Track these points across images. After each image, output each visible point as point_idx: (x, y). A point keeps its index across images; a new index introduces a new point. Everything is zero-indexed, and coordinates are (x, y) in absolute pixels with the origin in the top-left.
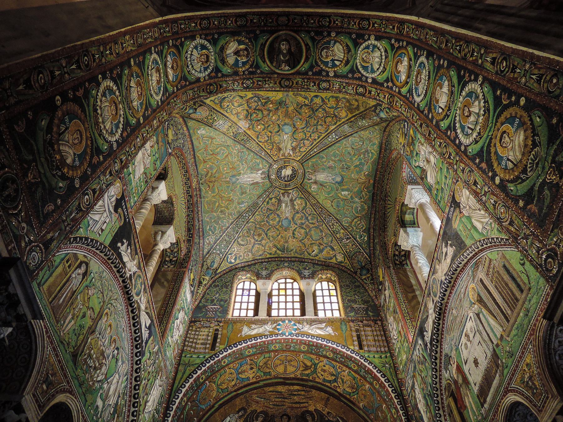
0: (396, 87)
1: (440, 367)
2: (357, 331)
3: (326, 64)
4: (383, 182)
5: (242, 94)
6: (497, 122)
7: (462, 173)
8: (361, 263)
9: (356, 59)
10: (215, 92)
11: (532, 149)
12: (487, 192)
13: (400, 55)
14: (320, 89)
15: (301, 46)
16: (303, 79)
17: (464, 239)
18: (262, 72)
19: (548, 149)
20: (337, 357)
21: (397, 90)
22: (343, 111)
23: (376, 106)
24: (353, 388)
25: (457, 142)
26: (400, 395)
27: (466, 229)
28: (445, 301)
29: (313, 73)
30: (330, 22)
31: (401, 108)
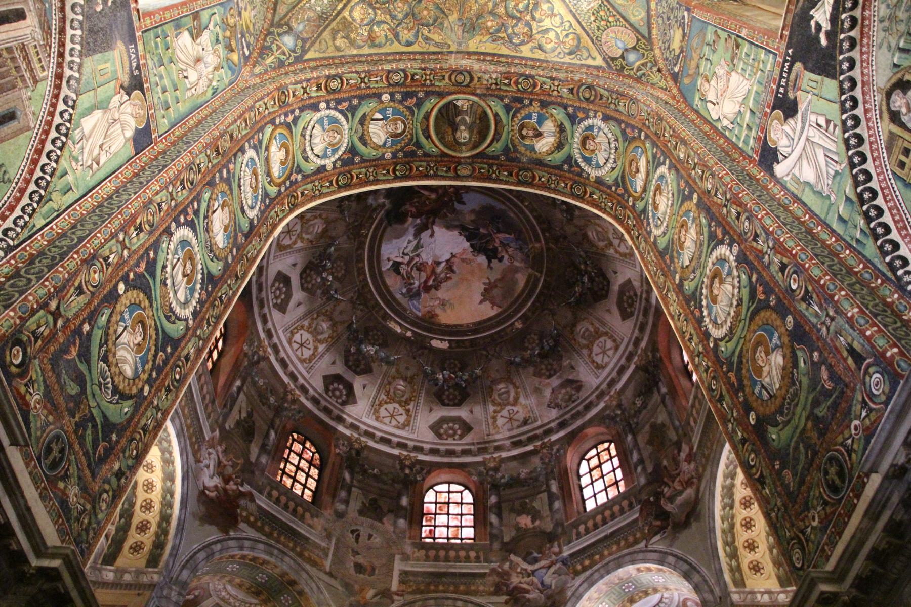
3: (396, 112)
5: (538, 55)
6: (156, 329)
10: (583, 84)
13: (284, 170)
14: (404, 71)
15: (437, 134)
16: (432, 85)
18: (501, 98)
19: (103, 413)
21: (277, 122)
22: (359, 21)
23: (304, 51)
25: (182, 219)
29: (416, 96)
30: (394, 171)
31: (266, 104)
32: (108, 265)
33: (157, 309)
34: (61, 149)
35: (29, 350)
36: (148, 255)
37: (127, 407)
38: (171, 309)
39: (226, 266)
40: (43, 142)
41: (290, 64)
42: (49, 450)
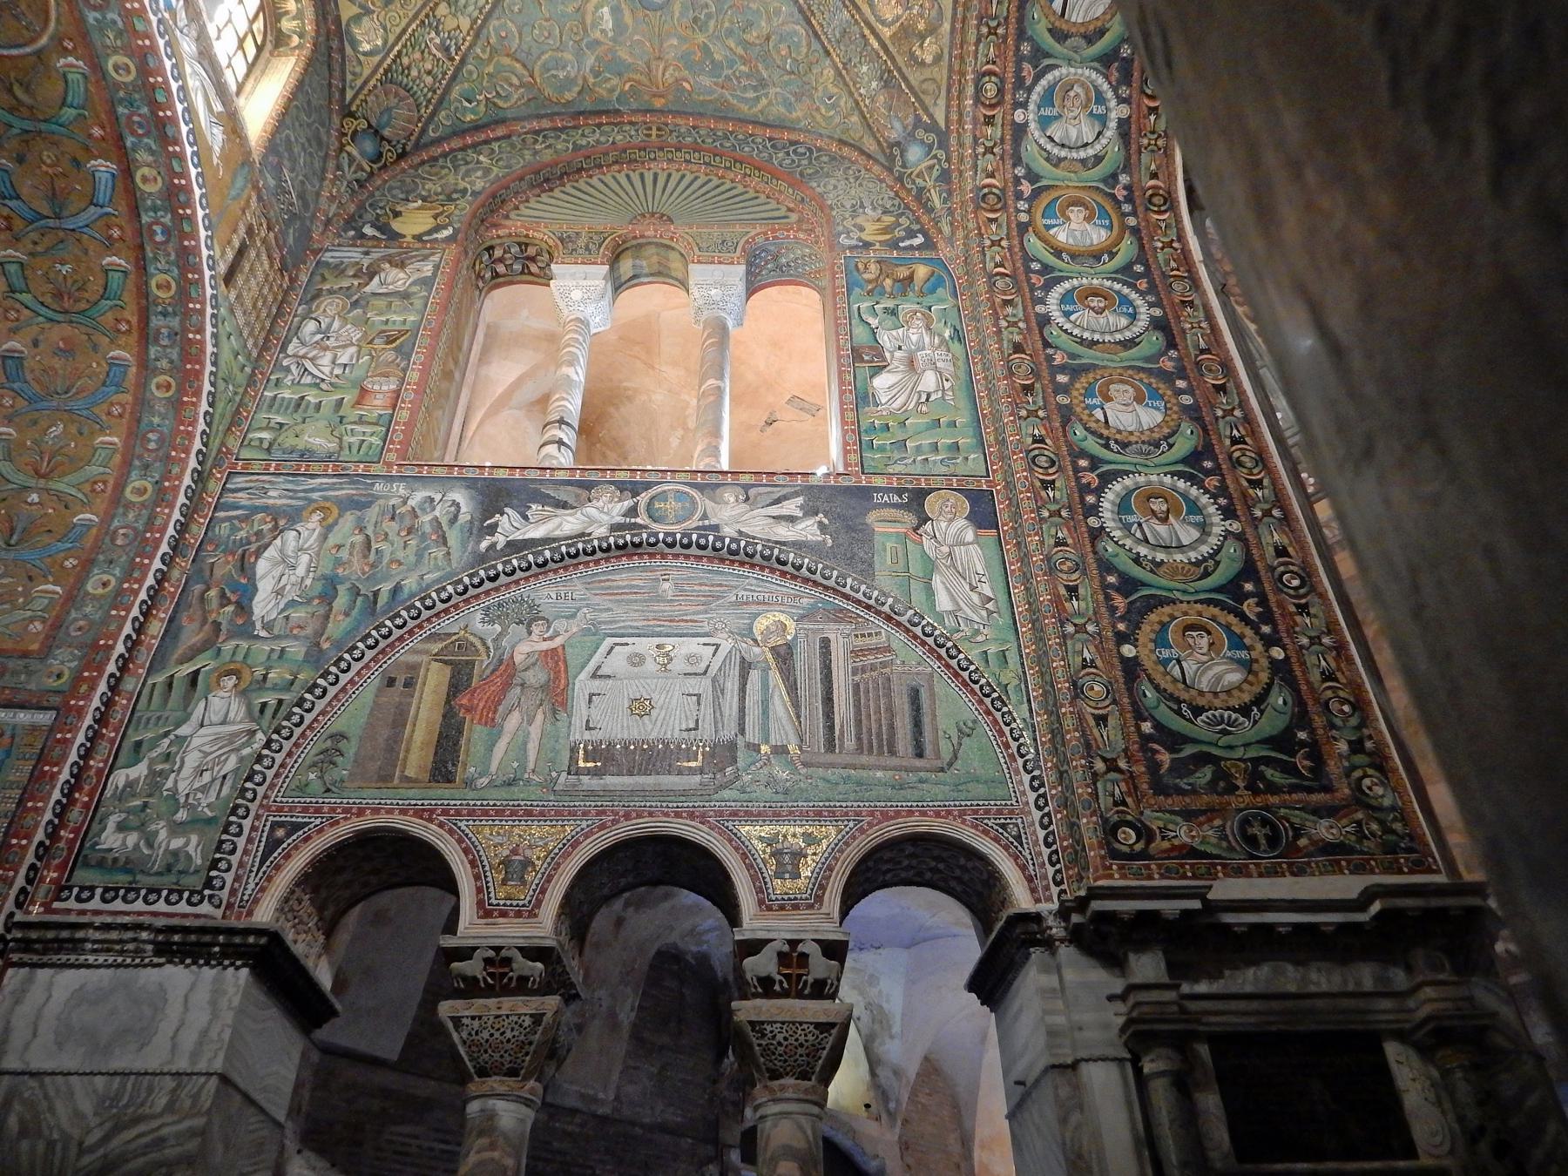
0: (1029, 211)
1: (477, 597)
2: (250, 231)
4: (678, 149)
6: (1208, 602)
7: (1052, 541)
8: (388, 124)
9: (1070, 62)
11: (1234, 710)
12: (1087, 633)
13: (1104, 214)
17: (877, 566)
19: (1258, 742)
20: (155, 209)
21: (1024, 218)
23: (932, 127)
24: (58, 295)
25: (1090, 499)
26: (200, 477)
27: (902, 562)
28: (667, 550)
31: (993, 243)
32: (1093, 664)
33: (1185, 592)
34: (960, 652)
35: (1129, 818)
36: (1111, 586)
37: (1278, 699)
38: (1198, 564)
39: (1194, 413)
40: (948, 666)
41: (948, 160)
42: (1252, 841)
